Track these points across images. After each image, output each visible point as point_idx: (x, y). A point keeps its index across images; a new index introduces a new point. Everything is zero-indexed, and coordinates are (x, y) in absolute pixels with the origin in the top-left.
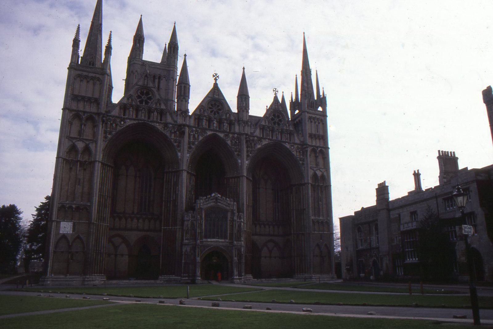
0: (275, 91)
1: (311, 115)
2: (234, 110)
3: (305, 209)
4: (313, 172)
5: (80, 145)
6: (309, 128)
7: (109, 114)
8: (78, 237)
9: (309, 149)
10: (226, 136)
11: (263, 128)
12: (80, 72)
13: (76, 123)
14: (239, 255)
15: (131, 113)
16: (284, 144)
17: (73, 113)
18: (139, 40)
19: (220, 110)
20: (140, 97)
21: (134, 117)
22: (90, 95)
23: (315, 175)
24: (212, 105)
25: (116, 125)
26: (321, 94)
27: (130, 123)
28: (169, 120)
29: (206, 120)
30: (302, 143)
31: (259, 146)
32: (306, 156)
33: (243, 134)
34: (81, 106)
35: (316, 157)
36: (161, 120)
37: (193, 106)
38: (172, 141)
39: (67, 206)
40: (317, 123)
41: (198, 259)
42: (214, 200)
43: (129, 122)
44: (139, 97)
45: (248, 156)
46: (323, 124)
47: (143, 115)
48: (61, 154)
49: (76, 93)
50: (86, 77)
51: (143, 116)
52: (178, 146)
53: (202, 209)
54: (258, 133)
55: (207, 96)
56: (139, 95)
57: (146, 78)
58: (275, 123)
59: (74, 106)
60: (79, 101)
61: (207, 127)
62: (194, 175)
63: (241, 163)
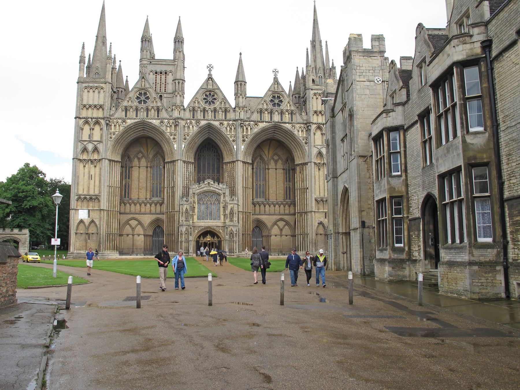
0: (275, 72)
1: (316, 92)
3: (308, 188)
4: (317, 150)
5: (90, 147)
8: (92, 221)
9: (314, 127)
10: (221, 124)
11: (261, 112)
12: (86, 85)
13: (87, 128)
15: (132, 113)
18: (146, 40)
22: (96, 103)
23: (320, 154)
24: (206, 95)
27: (130, 123)
29: (201, 111)
30: (305, 122)
31: (256, 130)
35: (322, 134)
36: (158, 116)
38: (168, 134)
39: (83, 197)
43: (129, 122)
44: (138, 98)
45: (244, 141)
49: (85, 103)
51: (142, 115)
54: (256, 117)
55: (201, 88)
57: (143, 80)
58: (274, 105)
60: (87, 109)
62: (192, 163)
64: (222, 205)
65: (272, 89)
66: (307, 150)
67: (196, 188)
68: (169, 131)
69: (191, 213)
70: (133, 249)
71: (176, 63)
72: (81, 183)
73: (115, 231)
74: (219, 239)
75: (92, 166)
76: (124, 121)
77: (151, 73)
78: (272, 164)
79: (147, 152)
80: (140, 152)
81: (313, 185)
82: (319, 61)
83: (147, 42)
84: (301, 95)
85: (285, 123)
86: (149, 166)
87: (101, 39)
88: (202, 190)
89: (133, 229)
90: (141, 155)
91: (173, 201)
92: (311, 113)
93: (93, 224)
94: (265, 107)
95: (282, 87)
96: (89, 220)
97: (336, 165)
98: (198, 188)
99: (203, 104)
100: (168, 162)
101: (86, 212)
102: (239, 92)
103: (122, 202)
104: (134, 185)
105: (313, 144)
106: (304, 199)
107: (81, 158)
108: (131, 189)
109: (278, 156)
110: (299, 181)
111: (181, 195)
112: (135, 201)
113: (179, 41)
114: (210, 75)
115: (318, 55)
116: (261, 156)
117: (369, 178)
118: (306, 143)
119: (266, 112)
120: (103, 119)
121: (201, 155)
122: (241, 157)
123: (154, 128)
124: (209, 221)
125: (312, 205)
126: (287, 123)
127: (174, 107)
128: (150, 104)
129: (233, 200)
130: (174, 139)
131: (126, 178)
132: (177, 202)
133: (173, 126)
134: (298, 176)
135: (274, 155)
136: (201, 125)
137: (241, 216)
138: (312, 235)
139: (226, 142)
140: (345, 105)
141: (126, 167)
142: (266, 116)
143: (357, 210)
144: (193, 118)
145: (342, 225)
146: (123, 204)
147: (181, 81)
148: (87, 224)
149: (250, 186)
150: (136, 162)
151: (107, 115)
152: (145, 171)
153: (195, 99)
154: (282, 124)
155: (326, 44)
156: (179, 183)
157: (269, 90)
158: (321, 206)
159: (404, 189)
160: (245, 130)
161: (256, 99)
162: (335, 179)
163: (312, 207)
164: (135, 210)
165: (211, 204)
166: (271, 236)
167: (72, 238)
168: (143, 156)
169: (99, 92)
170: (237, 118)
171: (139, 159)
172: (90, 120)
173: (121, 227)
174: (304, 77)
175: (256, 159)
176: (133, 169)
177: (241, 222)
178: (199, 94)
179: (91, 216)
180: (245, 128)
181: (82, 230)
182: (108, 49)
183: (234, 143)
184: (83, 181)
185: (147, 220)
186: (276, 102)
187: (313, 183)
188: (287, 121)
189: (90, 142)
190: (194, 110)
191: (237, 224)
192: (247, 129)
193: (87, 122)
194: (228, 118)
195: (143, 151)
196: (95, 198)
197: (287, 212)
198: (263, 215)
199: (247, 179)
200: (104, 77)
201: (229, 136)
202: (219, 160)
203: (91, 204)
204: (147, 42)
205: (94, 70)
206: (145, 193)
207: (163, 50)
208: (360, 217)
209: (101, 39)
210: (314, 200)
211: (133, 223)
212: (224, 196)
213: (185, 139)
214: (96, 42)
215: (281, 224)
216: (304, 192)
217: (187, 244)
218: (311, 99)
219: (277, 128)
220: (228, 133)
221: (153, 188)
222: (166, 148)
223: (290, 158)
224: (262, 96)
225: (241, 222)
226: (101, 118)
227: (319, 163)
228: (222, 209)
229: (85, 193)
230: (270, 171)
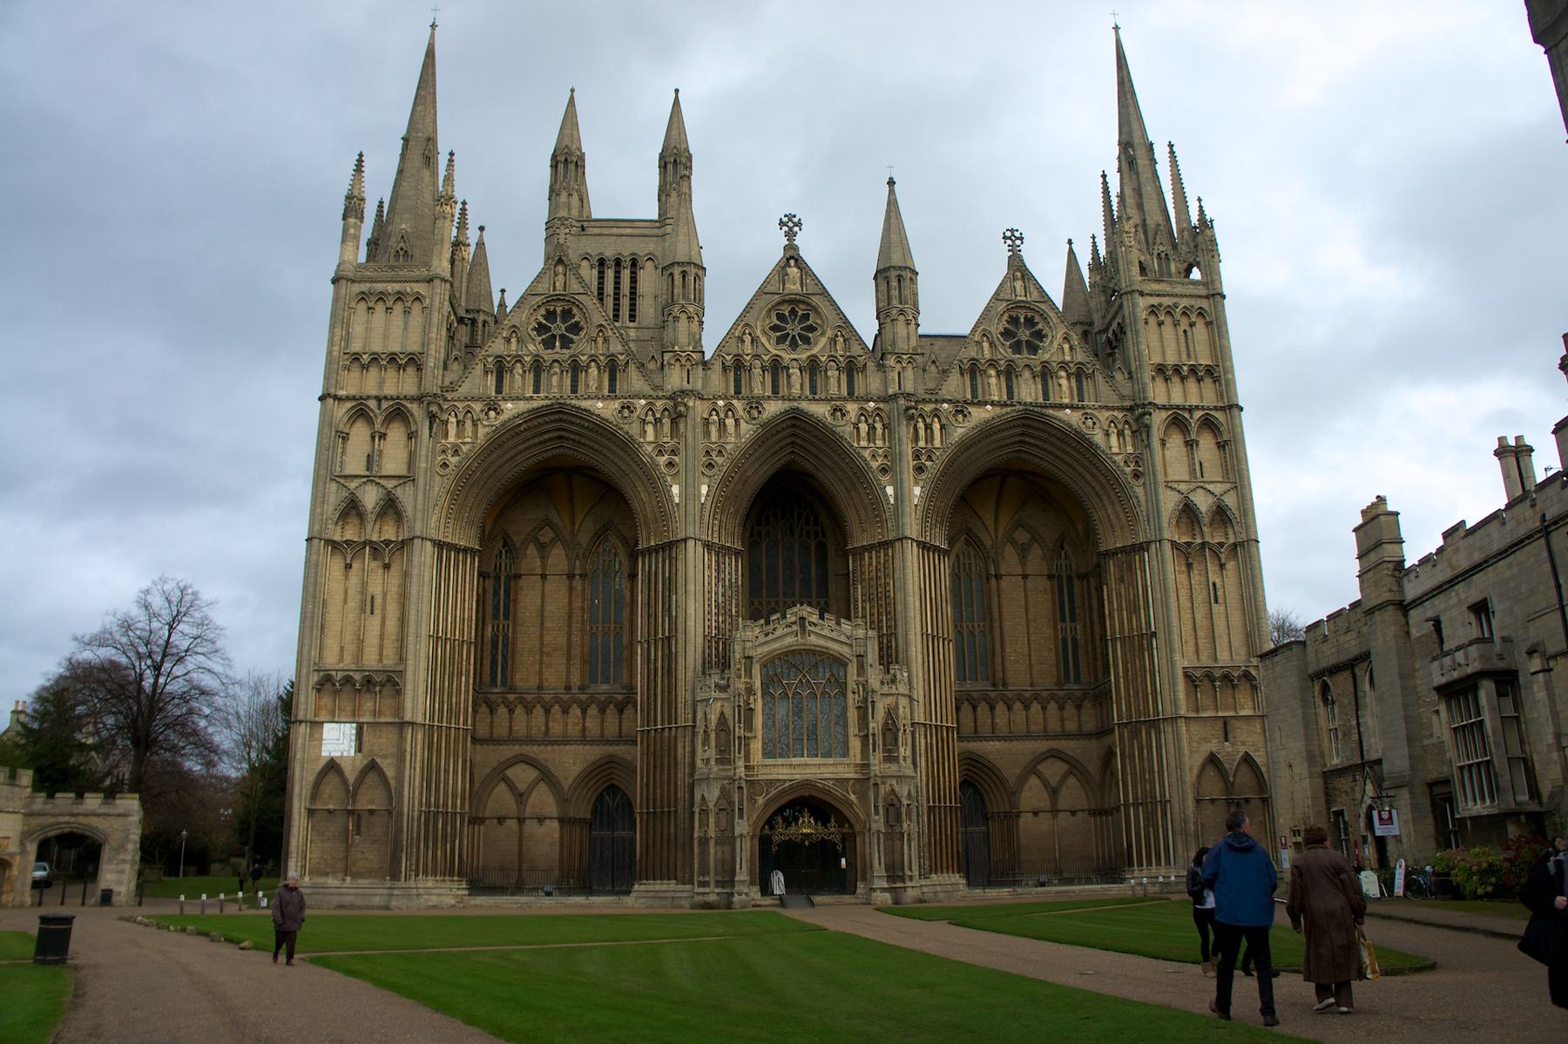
0: (1013, 239)
1: (1155, 301)
2: (866, 326)
4: (1176, 497)
5: (370, 498)
6: (1156, 344)
7: (455, 395)
8: (373, 766)
9: (1158, 419)
11: (974, 370)
13: (360, 432)
15: (519, 381)
16: (1059, 414)
17: (349, 405)
18: (567, 164)
19: (811, 329)
20: (549, 329)
21: (529, 393)
22: (396, 348)
23: (1188, 512)
24: (780, 317)
25: (475, 424)
26: (1194, 220)
30: (1127, 403)
31: (960, 431)
32: (1148, 446)
33: (894, 397)
34: (371, 383)
35: (1190, 445)
36: (612, 389)
37: (714, 332)
40: (1184, 324)
41: (742, 827)
42: (795, 628)
44: (541, 329)
45: (920, 469)
46: (1208, 324)
47: (555, 379)
48: (317, 527)
49: (356, 347)
50: (381, 297)
51: (556, 386)
54: (955, 386)
55: (762, 292)
56: (540, 324)
57: (560, 269)
58: (1017, 347)
59: (352, 384)
60: (365, 367)
61: (769, 393)
62: (737, 553)
63: (896, 499)
66: (1142, 499)
68: (650, 436)
70: (520, 870)
71: (669, 229)
72: (334, 627)
73: (454, 806)
74: (846, 830)
75: (374, 564)
76: (493, 406)
77: (585, 263)
79: (573, 523)
80: (548, 523)
81: (1175, 621)
82: (1151, 206)
83: (572, 167)
84: (1098, 326)
85: (1062, 407)
86: (578, 572)
87: (420, 146)
88: (776, 645)
89: (520, 797)
90: (552, 535)
91: (671, 689)
92: (1148, 374)
93: (372, 777)
94: (987, 354)
96: (361, 762)
98: (762, 639)
99: (770, 347)
100: (649, 551)
101: (349, 730)
102: (895, 302)
103: (483, 700)
104: (526, 639)
105: (1161, 478)
107: (337, 538)
108: (513, 654)
110: (1120, 610)
111: (699, 668)
112: (529, 698)
113: (675, 164)
115: (1148, 189)
116: (970, 533)
118: (1137, 476)
119: (993, 372)
120: (419, 399)
121: (760, 535)
122: (912, 526)
123: (600, 430)
124: (805, 760)
126: (1067, 407)
127: (667, 356)
128: (583, 347)
129: (893, 681)
130: (670, 464)
132: (682, 694)
133: (666, 421)
134: (1113, 594)
136: (765, 416)
139: (857, 475)
141: (498, 578)
142: (994, 386)
144: (738, 391)
146: (484, 709)
147: (692, 271)
148: (351, 777)
150: (531, 559)
151: (432, 383)
152: (564, 592)
154: (1051, 412)
155: (1172, 153)
156: (691, 623)
157: (996, 297)
158: (1204, 697)
160: (922, 433)
163: (1175, 702)
164: (529, 728)
165: (813, 695)
166: (1018, 816)
167: (295, 830)
168: (558, 538)
169: (407, 312)
170: (891, 392)
171: (543, 548)
172: (372, 404)
173: (478, 791)
174: (1096, 265)
176: (522, 583)
178: (754, 312)
179: (365, 748)
180: (921, 425)
181: (331, 799)
182: (442, 172)
183: (884, 479)
184: (340, 619)
185: (571, 762)
186: (1024, 338)
187: (1174, 613)
188: (1066, 401)
189: (370, 479)
190: (738, 367)
191: (910, 772)
192: (928, 427)
193: (361, 412)
194: (860, 390)
195: (555, 518)
196: (388, 683)
197: (1071, 726)
198: (987, 739)
199: (936, 610)
200: (428, 266)
201: (866, 454)
202: (822, 549)
203: (368, 705)
204: (572, 167)
205: (394, 244)
206: (563, 668)
207: (622, 188)
209: (420, 146)
210: (1180, 673)
211: (522, 775)
212: (861, 669)
213: (710, 466)
214: (403, 156)
215: (1053, 770)
216: (1141, 649)
217: (727, 848)
218: (1141, 325)
219: (1031, 425)
220: (863, 443)
222: (640, 498)
226: (413, 399)
227: (1188, 544)
228: (853, 715)
229: (348, 662)
230: (1003, 584)
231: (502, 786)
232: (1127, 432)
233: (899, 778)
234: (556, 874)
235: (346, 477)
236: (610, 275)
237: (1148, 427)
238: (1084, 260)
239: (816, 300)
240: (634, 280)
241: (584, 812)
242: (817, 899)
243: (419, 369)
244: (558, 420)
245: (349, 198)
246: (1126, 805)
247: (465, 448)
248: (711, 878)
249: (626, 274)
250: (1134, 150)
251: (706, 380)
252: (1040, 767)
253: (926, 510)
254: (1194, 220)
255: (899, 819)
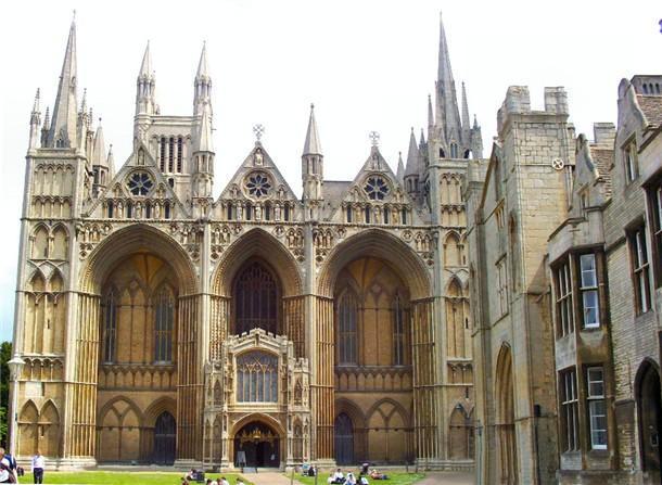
0: (374, 136)
1: (446, 171)
3: (434, 344)
4: (450, 275)
5: (47, 271)
8: (50, 402)
9: (443, 235)
11: (349, 208)
13: (41, 235)
14: (298, 428)
17: (36, 223)
18: (145, 84)
19: (268, 186)
23: (455, 282)
24: (252, 180)
25: (98, 234)
28: (180, 217)
30: (428, 226)
31: (340, 241)
33: (307, 223)
34: (45, 213)
35: (458, 247)
37: (217, 188)
41: (226, 435)
43: (115, 228)
45: (319, 259)
49: (38, 193)
52: (195, 256)
53: (230, 354)
54: (339, 217)
55: (243, 168)
61: (245, 220)
64: (281, 375)
65: (369, 168)
67: (234, 344)
69: (226, 389)
78: (370, 302)
79: (147, 278)
81: (444, 338)
82: (450, 116)
84: (421, 178)
85: (393, 228)
87: (67, 84)
88: (244, 348)
89: (120, 417)
90: (137, 284)
92: (439, 213)
95: (386, 165)
97: (488, 306)
100: (185, 298)
101: (40, 386)
102: (311, 173)
103: (102, 369)
104: (124, 337)
105: (442, 265)
106: (427, 362)
109: (380, 285)
112: (125, 367)
114: (259, 143)
115: (450, 107)
116: (349, 286)
117: (547, 330)
118: (430, 263)
122: (314, 289)
124: (257, 403)
125: (442, 376)
129: (300, 366)
131: (108, 326)
133: (194, 234)
135: (373, 283)
137: (314, 395)
138: (443, 427)
139: (289, 260)
140: (501, 204)
143: (526, 385)
145: (500, 412)
146: (102, 373)
149: (331, 341)
150: (126, 297)
153: (233, 187)
154: (389, 231)
157: (363, 170)
158: (459, 378)
159: (604, 351)
161: (341, 185)
162: (487, 332)
163: (441, 378)
165: (261, 373)
168: (140, 286)
171: (132, 293)
173: (100, 415)
175: (341, 290)
176: (123, 309)
177: (314, 405)
185: (146, 400)
189: (45, 262)
190: (229, 207)
195: (138, 276)
197: (397, 386)
208: (532, 397)
211: (121, 406)
215: (386, 408)
219: (377, 237)
221: (157, 342)
222: (181, 272)
223: (402, 290)
224: (351, 178)
225: (314, 405)
228: (280, 382)
231: (111, 412)
232: (427, 241)
233: (301, 413)
234: (137, 455)
235: (35, 260)
236: (168, 146)
237: (437, 239)
238: (418, 142)
239: (272, 172)
240: (180, 149)
241: (152, 425)
242: (259, 469)
243: (70, 205)
244: (139, 232)
245: (34, 113)
246: (417, 427)
247: (94, 247)
248: (211, 458)
249: (176, 147)
250: (444, 87)
251: (214, 214)
252: (381, 407)
253: (321, 281)
254: (472, 128)
255: (301, 433)
